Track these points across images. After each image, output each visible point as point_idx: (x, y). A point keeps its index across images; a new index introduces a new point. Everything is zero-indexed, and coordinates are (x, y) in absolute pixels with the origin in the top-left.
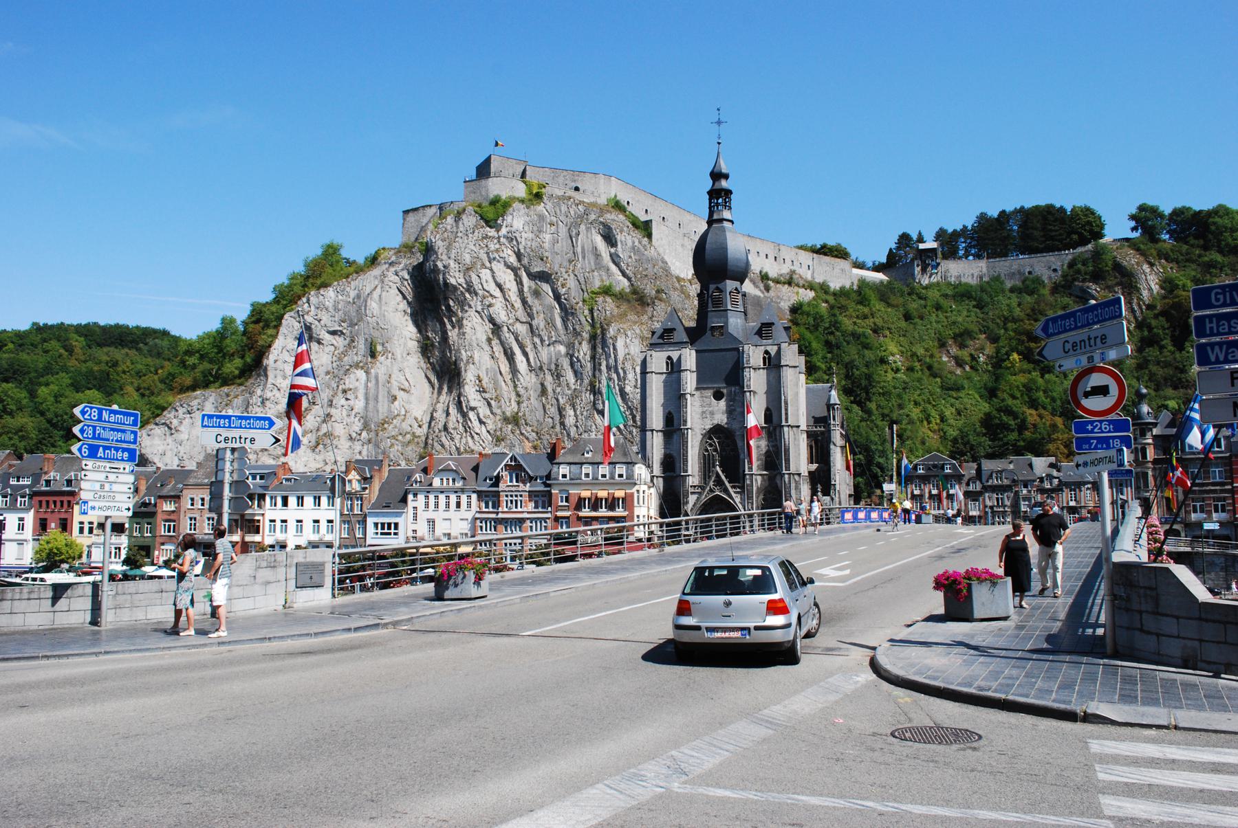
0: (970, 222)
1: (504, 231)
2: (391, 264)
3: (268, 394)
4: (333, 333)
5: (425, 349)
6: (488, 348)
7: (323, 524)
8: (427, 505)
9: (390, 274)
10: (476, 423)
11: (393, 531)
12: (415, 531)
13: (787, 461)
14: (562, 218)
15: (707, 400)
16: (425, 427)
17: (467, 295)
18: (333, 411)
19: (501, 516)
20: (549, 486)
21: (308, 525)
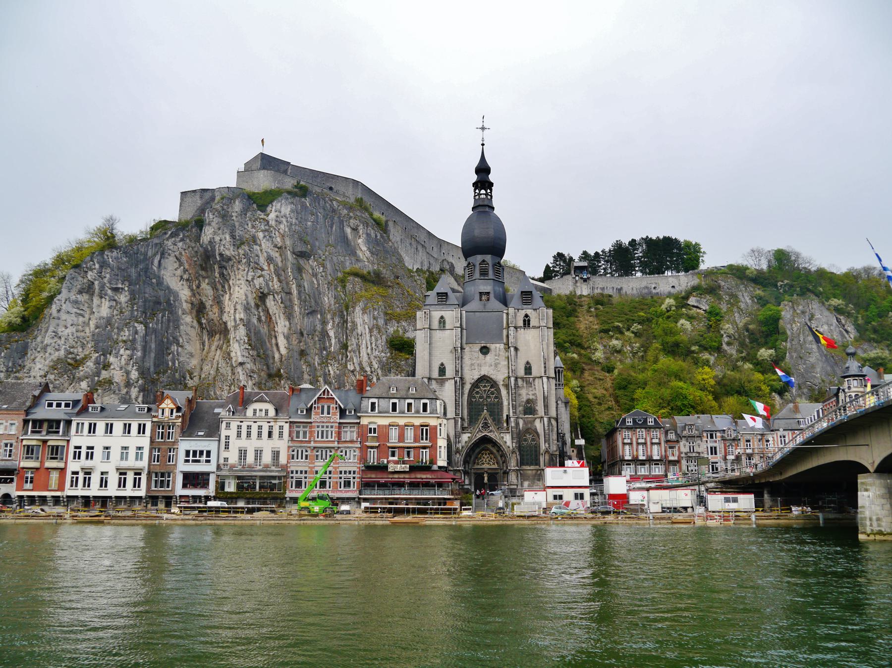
0: (608, 247)
1: (272, 216)
2: (172, 236)
3: (47, 340)
4: (116, 290)
5: (199, 310)
7: (132, 452)
8: (239, 435)
9: (169, 243)
10: (242, 377)
11: (204, 458)
12: (226, 459)
13: (546, 406)
14: (321, 211)
16: (196, 379)
18: (112, 359)
19: (312, 444)
20: (359, 418)
21: (115, 453)
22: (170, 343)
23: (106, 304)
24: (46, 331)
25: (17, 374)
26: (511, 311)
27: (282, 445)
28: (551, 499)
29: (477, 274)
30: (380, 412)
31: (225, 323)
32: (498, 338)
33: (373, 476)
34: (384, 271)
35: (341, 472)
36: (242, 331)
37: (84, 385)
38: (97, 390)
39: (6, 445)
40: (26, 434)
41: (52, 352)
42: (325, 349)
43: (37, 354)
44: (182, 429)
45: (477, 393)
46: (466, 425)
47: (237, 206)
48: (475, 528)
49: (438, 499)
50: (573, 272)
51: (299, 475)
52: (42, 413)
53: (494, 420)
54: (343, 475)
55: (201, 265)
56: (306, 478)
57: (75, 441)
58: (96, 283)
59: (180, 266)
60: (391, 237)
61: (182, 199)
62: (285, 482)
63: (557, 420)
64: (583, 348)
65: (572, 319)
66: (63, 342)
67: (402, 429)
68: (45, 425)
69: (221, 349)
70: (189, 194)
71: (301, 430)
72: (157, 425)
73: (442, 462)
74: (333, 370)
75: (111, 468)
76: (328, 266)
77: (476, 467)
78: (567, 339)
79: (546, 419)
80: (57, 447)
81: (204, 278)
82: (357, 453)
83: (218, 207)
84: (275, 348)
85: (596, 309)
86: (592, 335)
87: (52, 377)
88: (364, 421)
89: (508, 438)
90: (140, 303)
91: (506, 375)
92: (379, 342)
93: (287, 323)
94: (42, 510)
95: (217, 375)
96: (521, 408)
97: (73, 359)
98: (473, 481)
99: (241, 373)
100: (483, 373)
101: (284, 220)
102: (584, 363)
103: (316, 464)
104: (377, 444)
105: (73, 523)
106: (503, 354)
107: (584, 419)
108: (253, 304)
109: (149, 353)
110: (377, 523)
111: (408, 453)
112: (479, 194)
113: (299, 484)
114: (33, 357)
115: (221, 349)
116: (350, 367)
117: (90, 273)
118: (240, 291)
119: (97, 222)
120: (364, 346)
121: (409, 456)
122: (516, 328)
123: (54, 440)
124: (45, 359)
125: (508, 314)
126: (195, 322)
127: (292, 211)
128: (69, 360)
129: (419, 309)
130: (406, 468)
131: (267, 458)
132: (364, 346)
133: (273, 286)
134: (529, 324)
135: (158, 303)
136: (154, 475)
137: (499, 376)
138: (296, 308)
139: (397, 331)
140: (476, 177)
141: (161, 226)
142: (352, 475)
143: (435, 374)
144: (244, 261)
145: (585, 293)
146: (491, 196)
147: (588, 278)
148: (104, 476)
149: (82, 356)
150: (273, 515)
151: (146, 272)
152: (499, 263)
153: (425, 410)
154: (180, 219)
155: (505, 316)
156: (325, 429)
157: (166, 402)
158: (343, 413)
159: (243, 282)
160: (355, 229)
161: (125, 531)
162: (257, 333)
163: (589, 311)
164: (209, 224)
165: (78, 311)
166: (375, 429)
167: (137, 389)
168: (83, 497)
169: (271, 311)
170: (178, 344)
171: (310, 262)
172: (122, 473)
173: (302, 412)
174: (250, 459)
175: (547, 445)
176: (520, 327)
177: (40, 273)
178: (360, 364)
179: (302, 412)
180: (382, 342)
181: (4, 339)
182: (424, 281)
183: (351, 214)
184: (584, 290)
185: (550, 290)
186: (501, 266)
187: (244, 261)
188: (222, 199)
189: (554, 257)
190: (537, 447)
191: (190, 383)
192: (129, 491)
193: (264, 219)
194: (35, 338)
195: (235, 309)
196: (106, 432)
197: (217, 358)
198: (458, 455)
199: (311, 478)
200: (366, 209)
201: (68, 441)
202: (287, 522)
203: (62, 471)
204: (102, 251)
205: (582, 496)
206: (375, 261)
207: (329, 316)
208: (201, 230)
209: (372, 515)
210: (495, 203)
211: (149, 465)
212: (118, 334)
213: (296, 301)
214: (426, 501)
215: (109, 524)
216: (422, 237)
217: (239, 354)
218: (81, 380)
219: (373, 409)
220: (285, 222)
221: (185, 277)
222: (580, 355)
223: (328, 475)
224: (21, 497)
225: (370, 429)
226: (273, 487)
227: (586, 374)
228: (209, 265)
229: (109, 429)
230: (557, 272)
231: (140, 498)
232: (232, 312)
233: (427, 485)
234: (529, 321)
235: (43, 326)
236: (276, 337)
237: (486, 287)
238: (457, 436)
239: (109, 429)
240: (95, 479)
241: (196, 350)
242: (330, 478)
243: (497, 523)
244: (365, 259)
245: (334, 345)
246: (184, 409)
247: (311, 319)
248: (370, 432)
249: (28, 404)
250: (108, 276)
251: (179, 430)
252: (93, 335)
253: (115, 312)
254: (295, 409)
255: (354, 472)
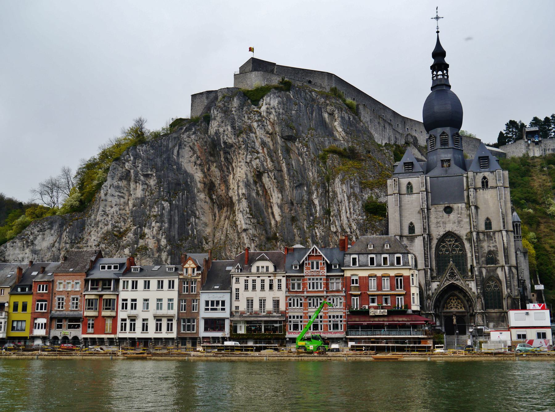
1: (264, 108)
2: (186, 130)
3: (99, 218)
4: (147, 176)
5: (210, 188)
6: (255, 188)
7: (165, 303)
8: (246, 288)
9: (185, 136)
10: (246, 241)
11: (220, 307)
12: (237, 307)
13: (507, 256)
14: (303, 101)
15: (441, 214)
16: (210, 244)
17: (240, 151)
18: (146, 230)
19: (305, 294)
21: (153, 304)
22: (189, 216)
23: (140, 187)
24: (98, 211)
25: (78, 245)
26: (470, 174)
27: (281, 295)
28: (515, 338)
29: (438, 145)
30: (360, 266)
31: (231, 198)
32: (460, 199)
33: (357, 319)
34: (358, 147)
35: (330, 317)
36: (244, 204)
37: (127, 251)
38: (136, 255)
39: (73, 299)
40: (87, 290)
41: (103, 227)
42: (312, 215)
43: (92, 229)
44: (202, 284)
45: (444, 247)
46: (435, 275)
47: (236, 103)
48: (447, 363)
49: (413, 338)
50: (525, 137)
51: (296, 319)
52: (98, 274)
53: (459, 270)
54: (332, 319)
55: (210, 153)
56: (301, 322)
57: (123, 295)
58: (132, 171)
59: (194, 154)
60: (362, 118)
61: (192, 101)
62: (285, 326)
63: (517, 268)
64: (538, 203)
65: (526, 179)
66: (110, 219)
67: (379, 280)
68: (101, 284)
69: (229, 218)
70: (198, 97)
71: (296, 282)
72: (182, 281)
73: (415, 306)
74: (319, 232)
75: (149, 315)
76: (311, 146)
77: (445, 310)
78: (523, 197)
79: (507, 268)
80: (110, 300)
81: (213, 162)
82: (343, 300)
83: (220, 104)
84: (271, 217)
85: (548, 168)
86: (546, 192)
87: (103, 246)
88: (348, 274)
89: (473, 285)
90: (165, 186)
91: (469, 230)
92: (357, 207)
93: (280, 195)
94: (101, 349)
95: (226, 240)
96: (483, 259)
97: (117, 231)
98: (443, 323)
99: (245, 238)
100: (447, 230)
101: (273, 111)
102: (539, 217)
103: (309, 310)
104: (359, 293)
105: (123, 359)
106: (465, 212)
107: (542, 267)
108: (252, 181)
109: (174, 224)
110: (362, 358)
111: (386, 299)
112: (437, 75)
113: (296, 327)
114: (89, 231)
115: (229, 218)
116: (333, 229)
117: (127, 164)
118: (241, 172)
119: (130, 124)
120: (344, 211)
121: (386, 303)
122: (475, 189)
123: (108, 295)
124: (98, 233)
125: (467, 177)
126: (208, 198)
127: (279, 103)
128: (115, 233)
129: (389, 177)
130: (385, 312)
131: (269, 306)
132: (344, 211)
133: (267, 165)
134: (487, 185)
135: (178, 184)
136: (182, 321)
137: (463, 232)
138: (287, 183)
139: (371, 197)
140: (433, 60)
141: (178, 124)
142: (339, 319)
143: (406, 232)
144: (243, 146)
145: (537, 154)
146: (448, 76)
147: (540, 141)
148: (145, 322)
149: (124, 228)
150: (276, 352)
151: (168, 160)
152: (457, 134)
153: (398, 263)
154: (192, 117)
155: (465, 179)
156: (315, 281)
157: (189, 262)
158: (329, 268)
159: (243, 164)
160: (331, 114)
161: (163, 365)
162: (257, 204)
163: (541, 171)
164: (215, 119)
165: (120, 194)
166: (356, 280)
167: (166, 253)
168: (130, 338)
169: (266, 186)
170: (195, 217)
171: (296, 144)
172: (158, 319)
173: (296, 267)
174: (256, 306)
175: (509, 291)
176: (479, 188)
177: (91, 166)
178: (341, 226)
179: (296, 267)
180: (359, 207)
181: (68, 218)
182: (392, 154)
183: (328, 102)
184: (536, 152)
185: (505, 154)
186: (459, 136)
187: (243, 146)
188: (224, 97)
189: (507, 125)
190: (500, 292)
191: (206, 247)
192: (164, 334)
193: (257, 111)
194: (90, 217)
195: (238, 186)
196: (145, 288)
197: (226, 226)
198: (429, 301)
199: (305, 322)
200: (340, 97)
201: (118, 295)
202: (288, 358)
203: (114, 318)
204: (135, 146)
205: (544, 336)
206: (350, 139)
207: (314, 188)
208: (208, 124)
209: (358, 352)
210: (451, 82)
211: (178, 313)
212: (150, 211)
213: (286, 177)
214: (403, 341)
215: (150, 359)
216: (389, 117)
217: (243, 222)
218: (124, 247)
219: (354, 263)
220: (274, 113)
221: (198, 162)
222: (535, 209)
223: (319, 319)
224: (85, 339)
225: (353, 280)
226: (275, 329)
227: (542, 227)
228: (217, 153)
229: (147, 285)
230: (510, 137)
231: (173, 339)
232: (236, 188)
233: (403, 327)
234: (487, 182)
235: (95, 207)
236: (271, 207)
237: (447, 155)
238: (428, 284)
239: (147, 285)
240: (139, 324)
241: (209, 221)
242: (321, 322)
243: (466, 359)
244: (341, 139)
245: (319, 211)
246: (203, 268)
247: (299, 191)
248: (353, 283)
249: (87, 267)
250: (140, 165)
251: (199, 285)
252: (132, 212)
253: (147, 193)
254: (290, 265)
255: (341, 317)
